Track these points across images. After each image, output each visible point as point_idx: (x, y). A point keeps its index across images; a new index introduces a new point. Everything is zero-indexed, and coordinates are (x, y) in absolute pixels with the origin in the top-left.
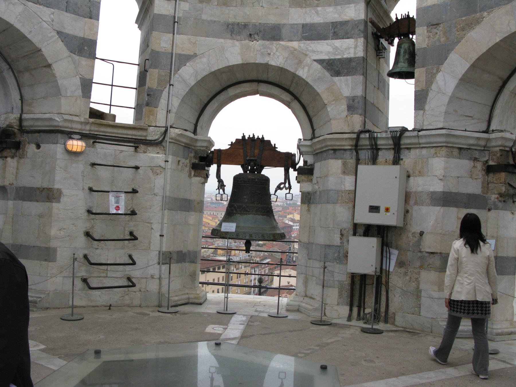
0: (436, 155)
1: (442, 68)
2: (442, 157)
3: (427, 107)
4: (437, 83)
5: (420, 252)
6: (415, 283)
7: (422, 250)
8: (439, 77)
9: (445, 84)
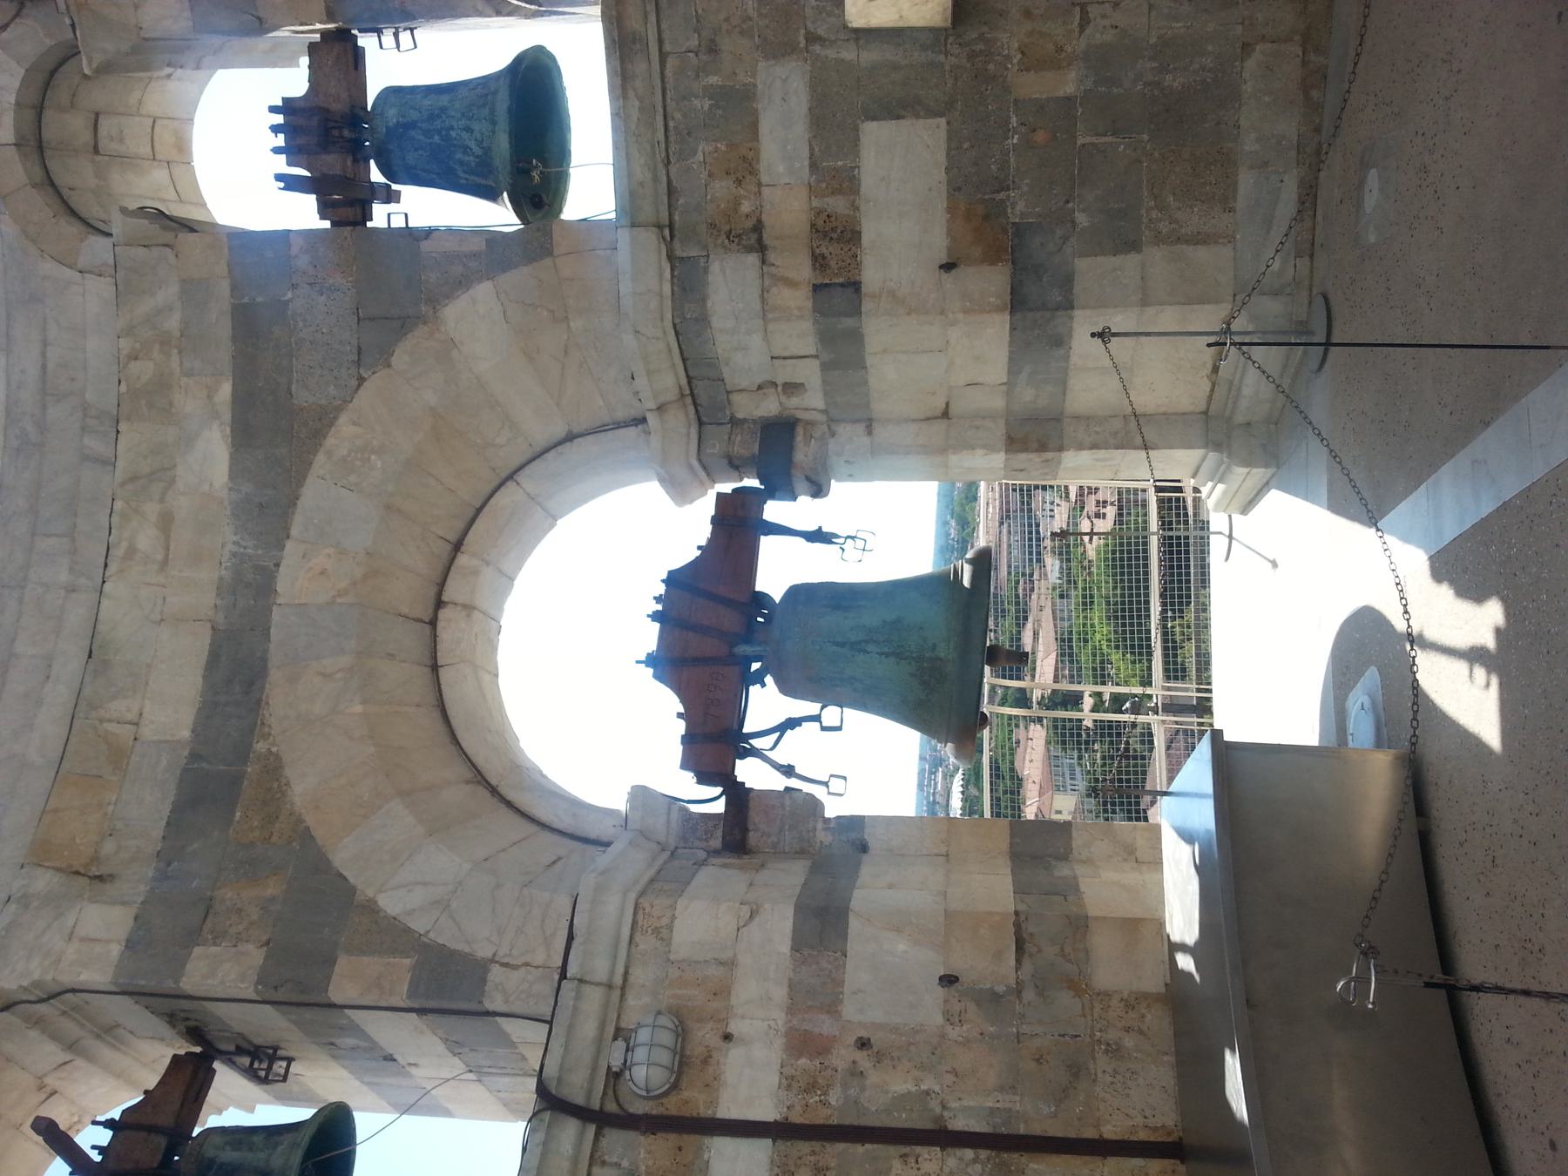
0: (663, 930)
1: (366, 890)
2: (673, 907)
3: (484, 951)
4: (410, 913)
5: (1018, 990)
6: (1143, 1011)
7: (1012, 982)
8: (391, 904)
9: (425, 884)
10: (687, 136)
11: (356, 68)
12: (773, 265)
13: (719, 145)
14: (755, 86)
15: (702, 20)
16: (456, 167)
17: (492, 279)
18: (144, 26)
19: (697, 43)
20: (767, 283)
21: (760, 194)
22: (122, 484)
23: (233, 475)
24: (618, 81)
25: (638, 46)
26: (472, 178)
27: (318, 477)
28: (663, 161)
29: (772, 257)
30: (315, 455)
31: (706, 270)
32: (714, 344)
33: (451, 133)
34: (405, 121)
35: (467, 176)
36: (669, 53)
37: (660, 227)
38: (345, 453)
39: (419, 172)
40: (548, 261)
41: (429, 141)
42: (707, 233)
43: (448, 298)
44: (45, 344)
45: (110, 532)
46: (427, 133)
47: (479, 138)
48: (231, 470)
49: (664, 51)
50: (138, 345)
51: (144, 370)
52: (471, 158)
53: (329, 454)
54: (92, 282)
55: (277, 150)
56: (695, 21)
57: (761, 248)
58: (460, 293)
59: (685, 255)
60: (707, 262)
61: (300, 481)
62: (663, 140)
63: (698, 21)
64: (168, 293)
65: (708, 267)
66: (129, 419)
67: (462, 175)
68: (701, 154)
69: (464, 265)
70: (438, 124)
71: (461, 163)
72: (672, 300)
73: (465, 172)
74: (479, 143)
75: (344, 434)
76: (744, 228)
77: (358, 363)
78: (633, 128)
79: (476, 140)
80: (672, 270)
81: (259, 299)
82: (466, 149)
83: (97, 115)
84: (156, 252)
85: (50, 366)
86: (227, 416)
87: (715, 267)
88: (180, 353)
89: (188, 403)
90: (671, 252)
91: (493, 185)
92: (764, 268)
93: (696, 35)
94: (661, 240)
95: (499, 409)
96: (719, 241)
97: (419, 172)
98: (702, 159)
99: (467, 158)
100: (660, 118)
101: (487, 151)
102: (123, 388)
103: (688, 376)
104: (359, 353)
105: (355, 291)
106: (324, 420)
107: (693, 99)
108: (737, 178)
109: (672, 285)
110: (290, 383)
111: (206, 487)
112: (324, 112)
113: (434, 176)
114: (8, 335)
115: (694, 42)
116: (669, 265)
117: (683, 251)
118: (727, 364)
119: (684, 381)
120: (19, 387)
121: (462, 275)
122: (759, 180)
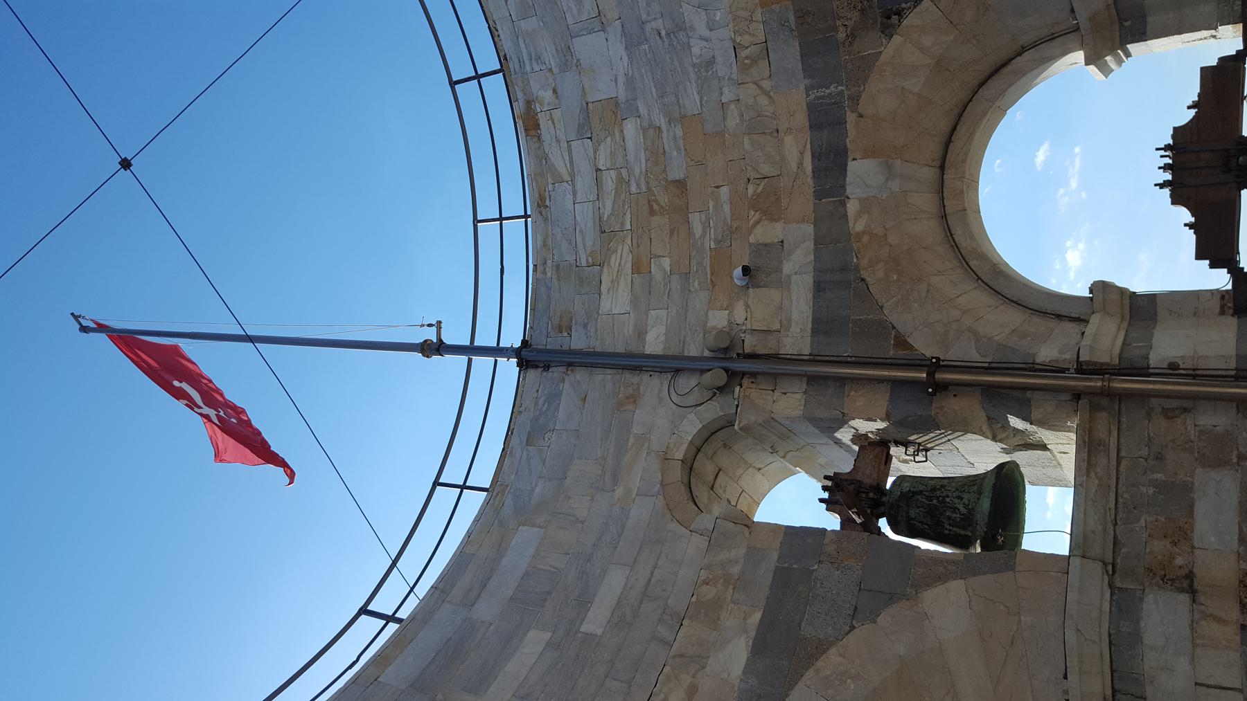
10: (1133, 510)
11: (886, 464)
12: (1203, 604)
13: (1159, 517)
14: (1192, 483)
15: (1152, 439)
16: (945, 521)
17: (965, 579)
18: (774, 411)
19: (1147, 453)
20: (1196, 616)
21: (1193, 554)
22: (674, 657)
23: (746, 671)
24: (1084, 465)
25: (1102, 447)
26: (955, 529)
27: (806, 685)
28: (1112, 521)
29: (1202, 599)
30: (806, 670)
31: (1141, 600)
32: (1142, 660)
33: (947, 499)
34: (915, 490)
35: (951, 528)
36: (1124, 457)
37: (1105, 564)
38: (829, 673)
39: (916, 523)
40: (1009, 574)
41: (928, 502)
42: (1144, 574)
43: (928, 586)
44: (655, 567)
45: (655, 686)
46: (929, 498)
47: (967, 502)
48: (745, 668)
49: (1120, 455)
50: (711, 577)
51: (710, 592)
52: (958, 515)
53: (818, 671)
54: (695, 537)
55: (821, 500)
56: (1147, 439)
57: (1192, 591)
58: (938, 584)
59: (1123, 586)
60: (1143, 594)
61: (792, 685)
62: (1114, 507)
63: (1149, 440)
64: (739, 552)
65: (1143, 597)
66: (690, 619)
67: (948, 527)
68: (1144, 522)
69: (945, 567)
70: (938, 493)
71: (949, 518)
72: (1110, 617)
73: (950, 525)
74: (966, 506)
75: (831, 661)
76: (1177, 575)
77: (853, 616)
78: (1092, 495)
79: (964, 504)
80: (1112, 595)
81: (795, 566)
82: (955, 510)
83: (720, 470)
84: (740, 527)
85: (653, 580)
86: (753, 634)
87: (1149, 599)
88: (734, 589)
89: (730, 621)
90: (1112, 583)
91: (970, 534)
92: (1194, 605)
93: (1147, 448)
94: (1105, 572)
95: (949, 677)
96: (1155, 581)
97: (916, 523)
98: (1144, 525)
99: (955, 515)
100: (1113, 494)
101: (971, 511)
102: (694, 599)
103: (1113, 688)
104: (855, 611)
105: (861, 571)
106: (820, 648)
107: (1140, 486)
108: (1173, 541)
109: (1111, 605)
110: (801, 620)
111: (725, 675)
112: (858, 484)
113: (926, 527)
114: (636, 558)
115: (1145, 452)
116: (1109, 591)
117: (1122, 584)
118: (1152, 682)
119: (1109, 692)
120: (631, 588)
121: (942, 573)
122: (1192, 544)
